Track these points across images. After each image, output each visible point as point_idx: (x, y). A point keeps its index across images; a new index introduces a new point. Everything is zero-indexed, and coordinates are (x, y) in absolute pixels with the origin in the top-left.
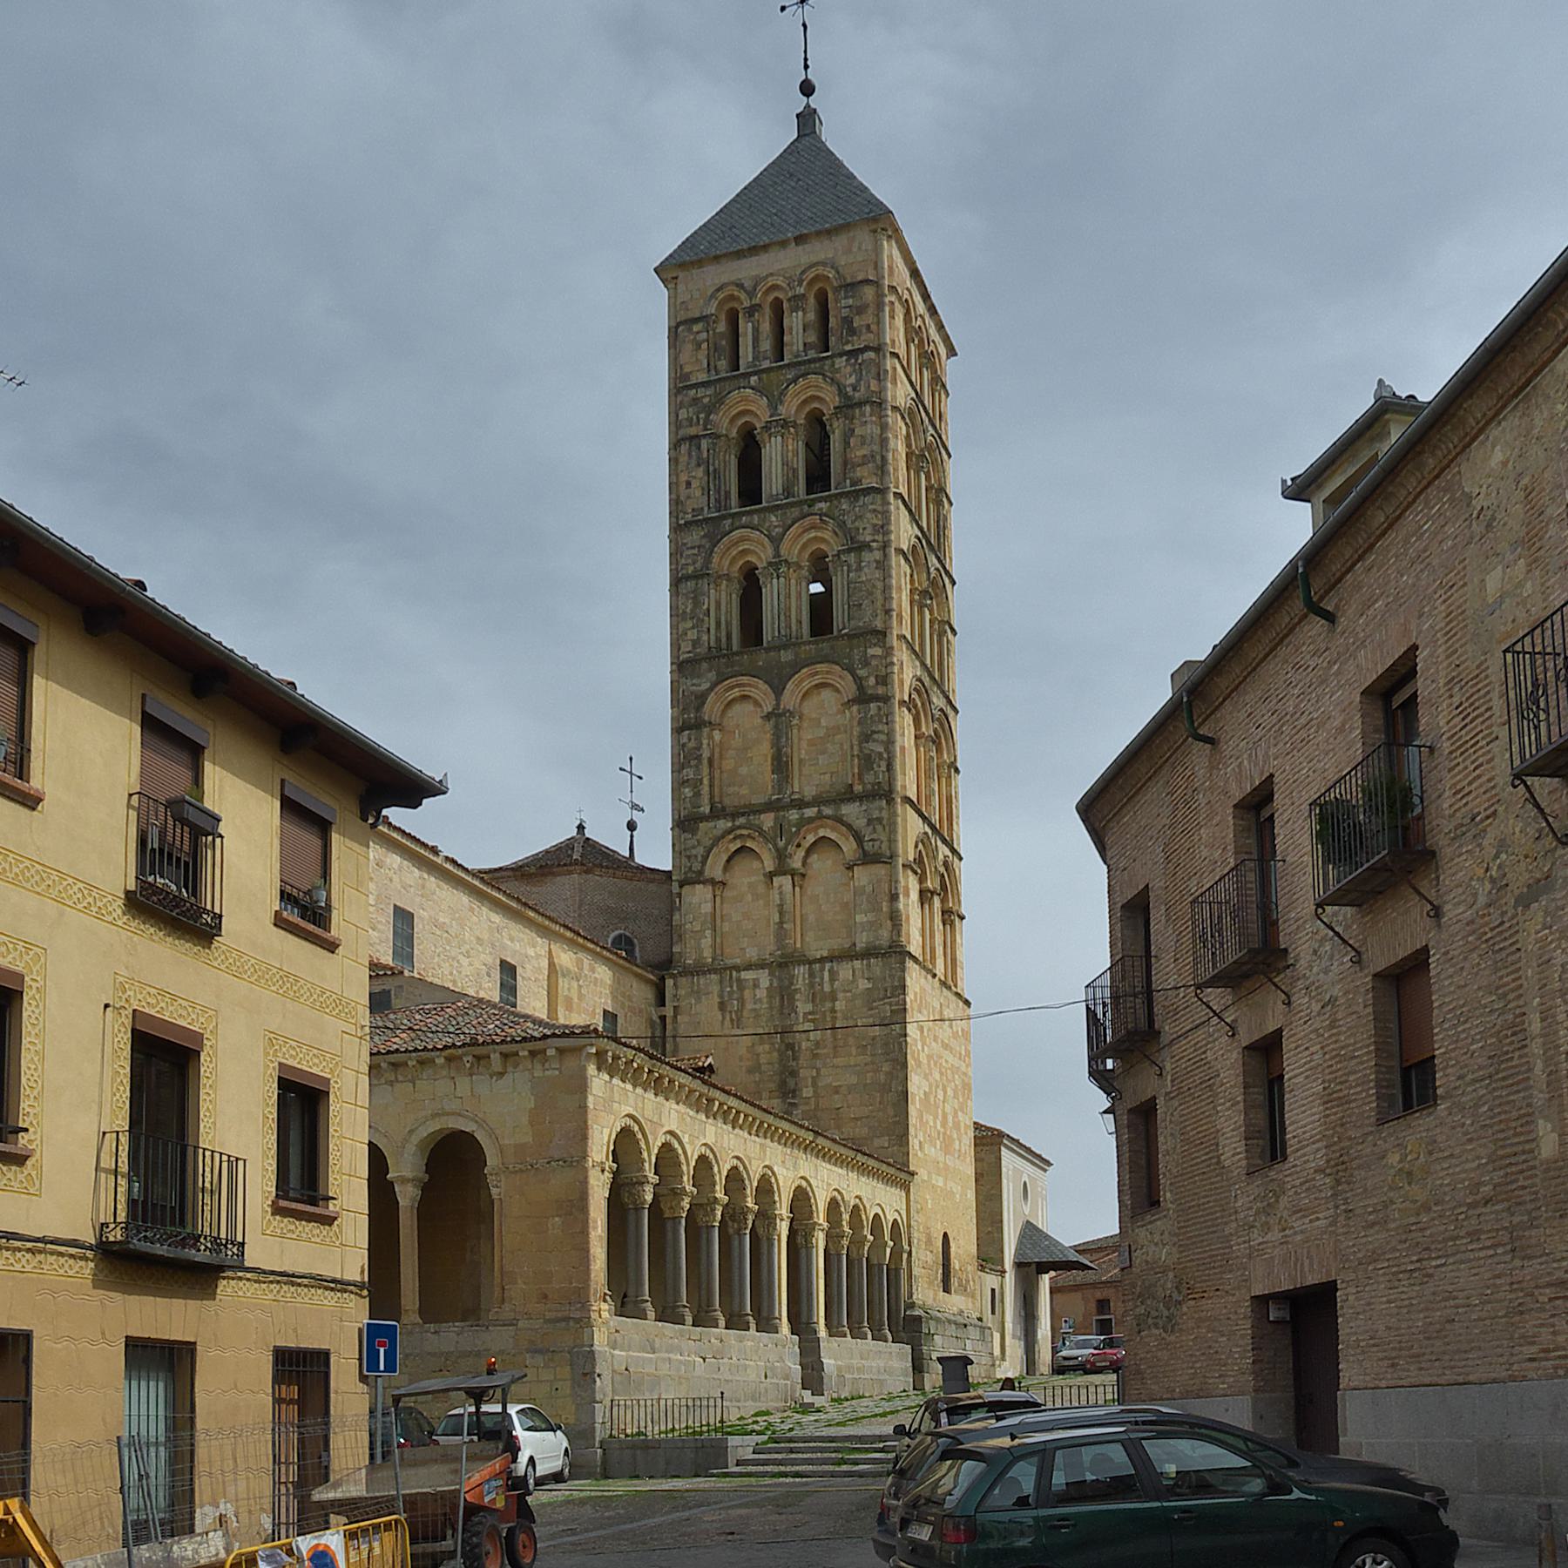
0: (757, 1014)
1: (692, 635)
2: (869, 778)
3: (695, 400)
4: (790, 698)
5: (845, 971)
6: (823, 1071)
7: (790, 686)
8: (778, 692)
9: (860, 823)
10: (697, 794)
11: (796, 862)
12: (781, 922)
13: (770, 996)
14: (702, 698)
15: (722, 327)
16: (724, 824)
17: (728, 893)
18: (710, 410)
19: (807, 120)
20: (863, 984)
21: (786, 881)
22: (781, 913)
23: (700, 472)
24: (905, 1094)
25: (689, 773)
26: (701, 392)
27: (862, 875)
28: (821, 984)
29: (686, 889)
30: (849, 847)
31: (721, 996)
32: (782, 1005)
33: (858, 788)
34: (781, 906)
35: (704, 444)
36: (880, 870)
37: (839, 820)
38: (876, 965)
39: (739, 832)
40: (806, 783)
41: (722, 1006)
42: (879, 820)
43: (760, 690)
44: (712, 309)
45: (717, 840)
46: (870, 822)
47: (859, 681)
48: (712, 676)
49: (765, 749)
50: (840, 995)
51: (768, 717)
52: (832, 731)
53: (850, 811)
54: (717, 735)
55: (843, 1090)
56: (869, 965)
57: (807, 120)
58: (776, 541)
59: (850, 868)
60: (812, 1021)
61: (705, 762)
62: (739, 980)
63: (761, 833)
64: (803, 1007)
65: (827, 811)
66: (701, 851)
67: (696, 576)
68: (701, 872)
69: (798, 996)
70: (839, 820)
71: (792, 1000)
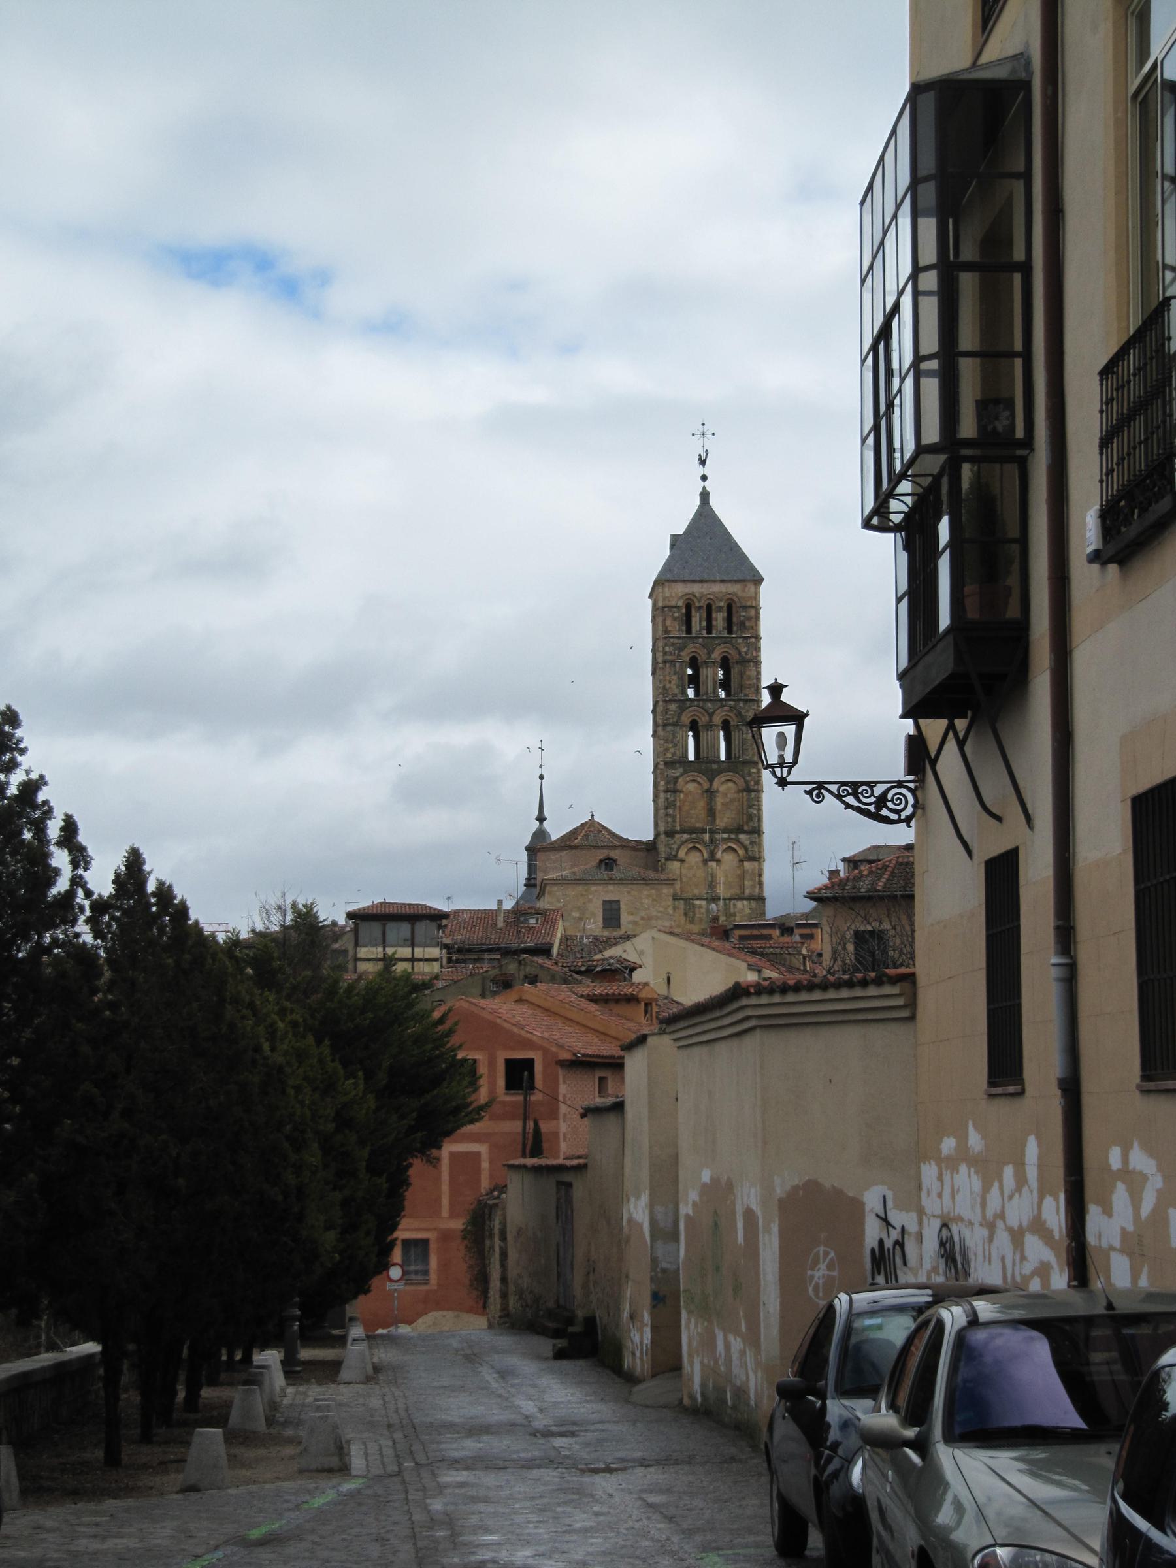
0: (701, 920)
1: (672, 750)
2: (751, 824)
3: (673, 644)
4: (716, 784)
5: (739, 904)
8: (711, 781)
9: (747, 843)
10: (674, 821)
14: (676, 779)
15: (684, 611)
16: (686, 836)
17: (686, 865)
18: (681, 649)
19: (705, 495)
21: (714, 864)
23: (675, 677)
25: (670, 811)
26: (676, 641)
27: (747, 865)
29: (669, 863)
30: (741, 852)
33: (746, 828)
35: (677, 665)
36: (756, 864)
37: (737, 841)
38: (753, 904)
40: (723, 821)
41: (685, 914)
43: (703, 779)
44: (680, 604)
45: (683, 843)
46: (752, 843)
47: (746, 782)
48: (681, 770)
49: (702, 803)
51: (707, 791)
52: (732, 801)
53: (742, 837)
54: (682, 795)
57: (705, 495)
58: (711, 715)
59: (742, 861)
62: (694, 906)
63: (704, 843)
65: (733, 836)
66: (675, 846)
67: (674, 724)
68: (676, 856)
70: (737, 841)
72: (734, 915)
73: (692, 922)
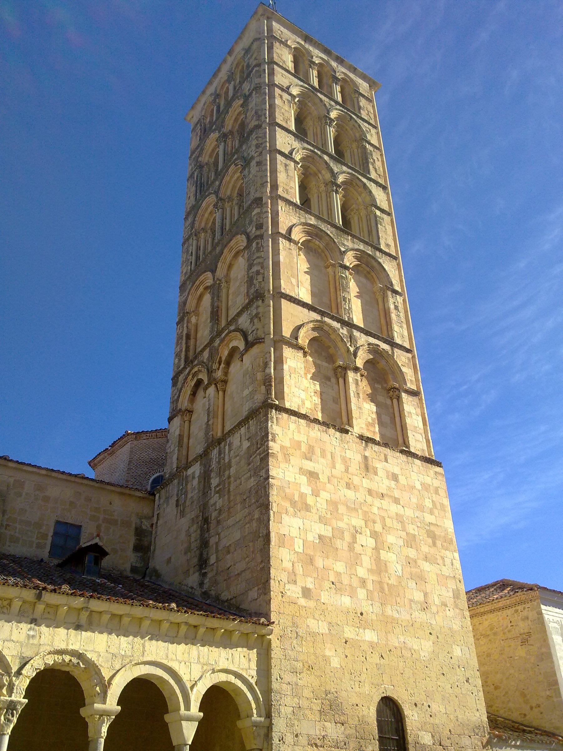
4: (221, 272)
6: (222, 535)
7: (219, 265)
11: (219, 374)
12: (208, 422)
13: (199, 482)
20: (246, 444)
22: (208, 415)
24: (268, 535)
28: (224, 459)
31: (177, 495)
32: (204, 488)
34: (209, 408)
39: (193, 371)
42: (257, 315)
50: (233, 461)
55: (232, 549)
56: (248, 428)
60: (218, 492)
61: (184, 338)
64: (214, 482)
69: (213, 475)
71: (209, 478)
72: (230, 466)
73: (182, 514)
